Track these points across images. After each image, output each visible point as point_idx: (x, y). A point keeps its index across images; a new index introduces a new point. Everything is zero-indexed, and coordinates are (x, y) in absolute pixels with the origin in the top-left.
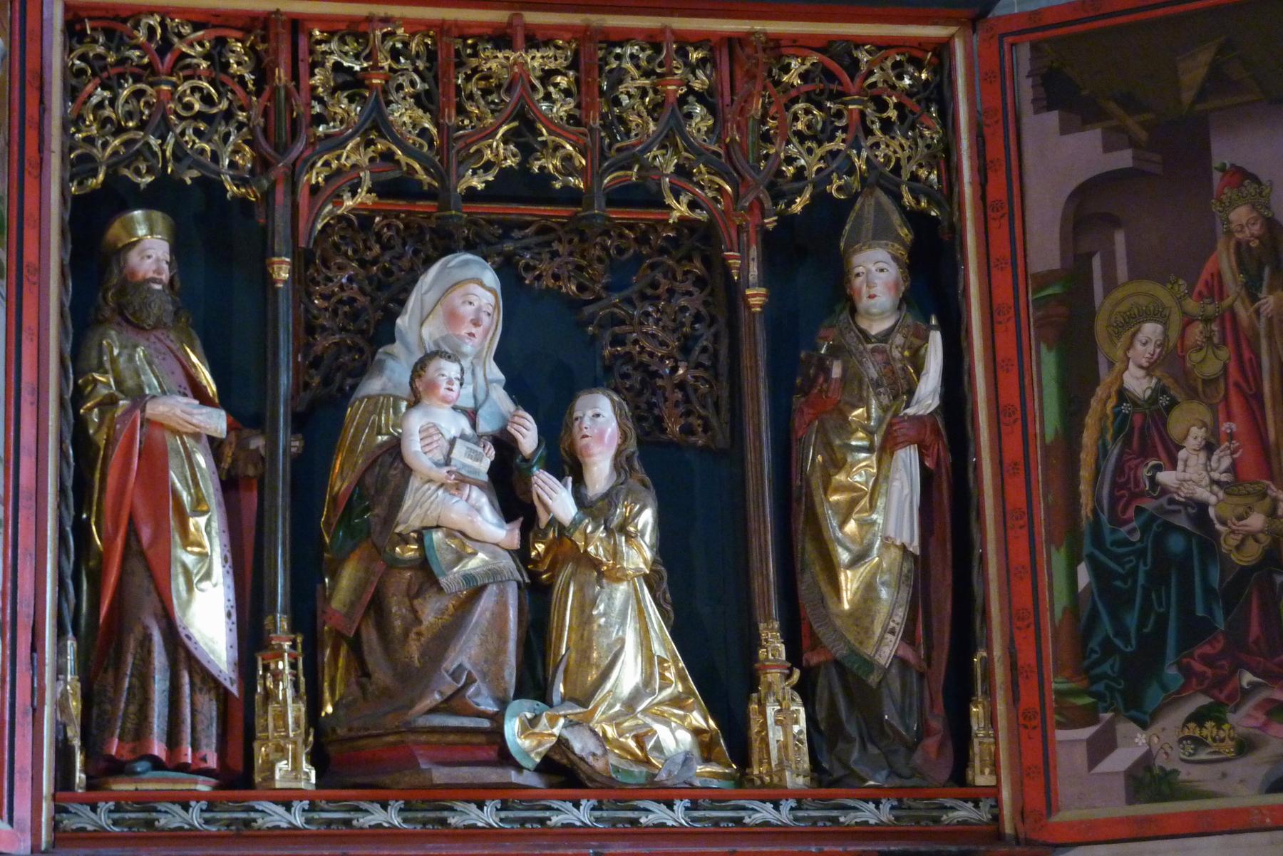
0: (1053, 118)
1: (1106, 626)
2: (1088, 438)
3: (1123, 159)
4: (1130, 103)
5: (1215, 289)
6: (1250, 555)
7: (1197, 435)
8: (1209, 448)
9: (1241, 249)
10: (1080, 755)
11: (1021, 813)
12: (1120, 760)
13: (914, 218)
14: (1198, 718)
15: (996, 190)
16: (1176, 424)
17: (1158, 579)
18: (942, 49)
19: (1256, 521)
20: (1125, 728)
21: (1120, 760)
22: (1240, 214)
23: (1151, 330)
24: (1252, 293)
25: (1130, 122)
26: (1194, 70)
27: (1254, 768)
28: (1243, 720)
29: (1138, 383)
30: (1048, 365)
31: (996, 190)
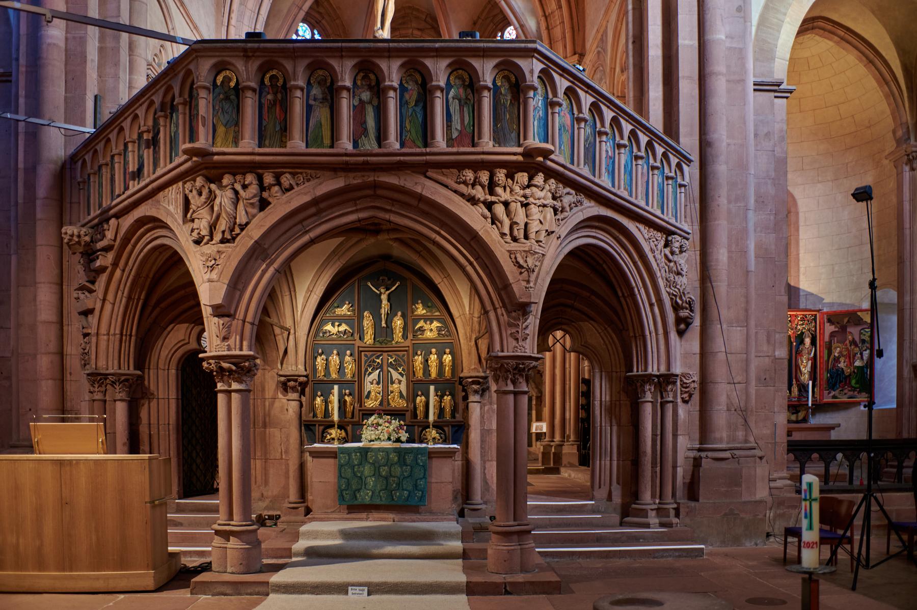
0: (829, 324)
1: (831, 380)
2: (830, 360)
3: (837, 329)
4: (838, 323)
5: (846, 345)
6: (848, 374)
7: (843, 361)
8: (844, 362)
9: (850, 341)
10: (826, 394)
11: (820, 399)
12: (831, 395)
13: (812, 334)
14: (841, 391)
15: (822, 332)
16: (840, 359)
17: (837, 376)
18: (816, 315)
19: (849, 371)
20: (832, 391)
21: (831, 395)
22: (850, 337)
23: (838, 349)
24: (851, 345)
25: (838, 325)
26: (846, 320)
27: (847, 396)
28: (846, 391)
29: (837, 355)
30: (826, 352)
31: (822, 332)
